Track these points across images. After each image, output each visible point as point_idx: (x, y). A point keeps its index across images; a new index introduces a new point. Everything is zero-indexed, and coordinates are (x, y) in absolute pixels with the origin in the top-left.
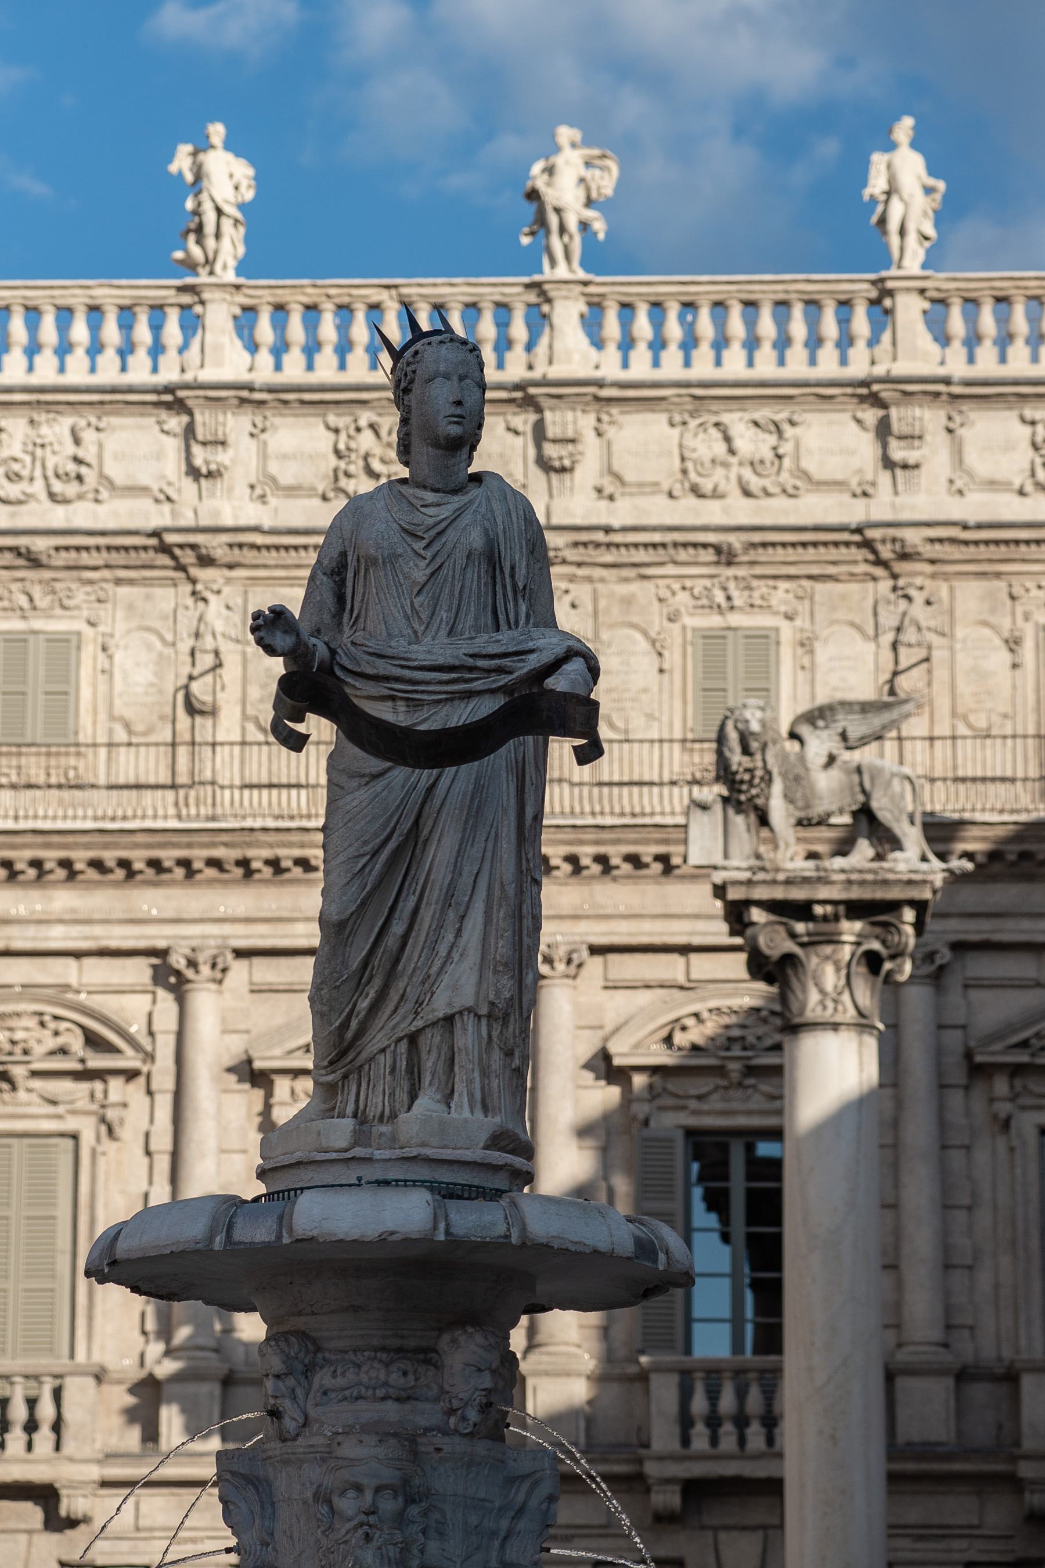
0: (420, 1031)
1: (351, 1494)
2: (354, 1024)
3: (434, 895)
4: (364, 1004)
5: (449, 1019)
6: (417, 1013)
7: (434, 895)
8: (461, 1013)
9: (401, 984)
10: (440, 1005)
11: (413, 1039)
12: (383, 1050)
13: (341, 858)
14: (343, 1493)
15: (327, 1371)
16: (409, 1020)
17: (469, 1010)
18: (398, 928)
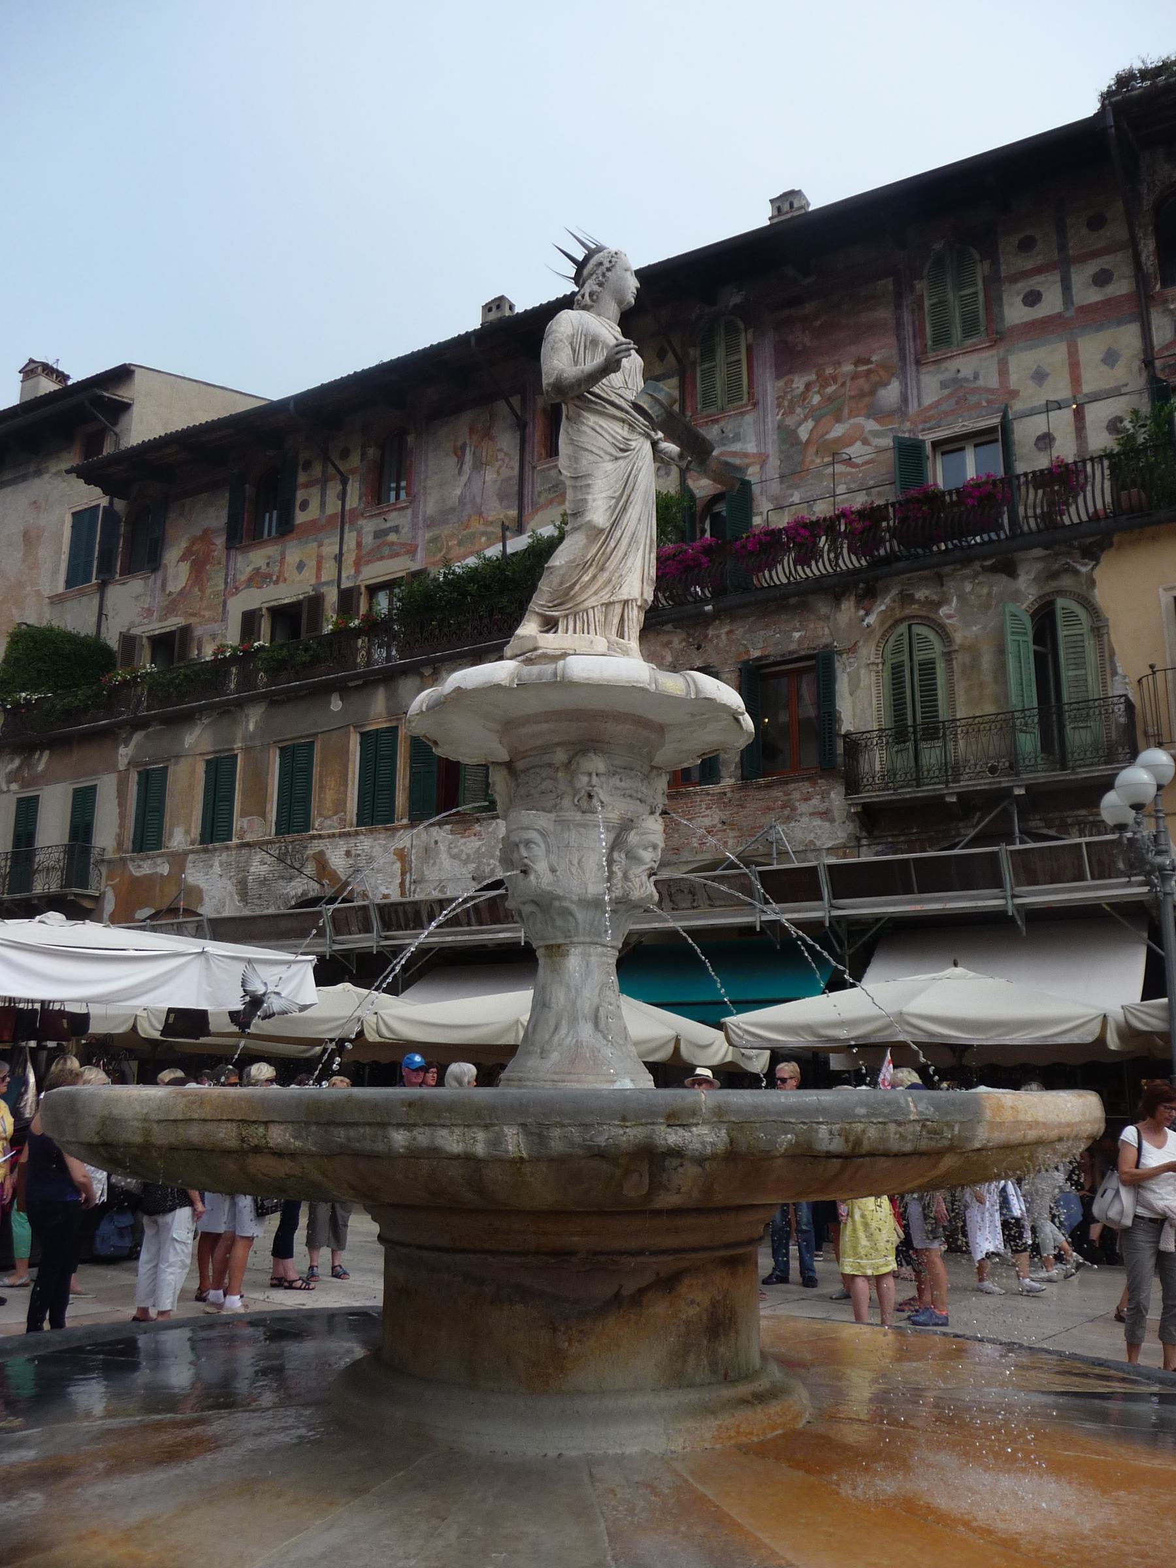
0: (614, 603)
1: (650, 849)
2: (577, 587)
3: (628, 534)
4: (586, 578)
5: (626, 602)
6: (613, 593)
7: (628, 534)
8: (632, 600)
9: (606, 575)
10: (624, 594)
11: (608, 605)
12: (593, 608)
13: (604, 495)
14: (645, 849)
15: (617, 777)
16: (609, 595)
17: (636, 600)
18: (612, 544)
